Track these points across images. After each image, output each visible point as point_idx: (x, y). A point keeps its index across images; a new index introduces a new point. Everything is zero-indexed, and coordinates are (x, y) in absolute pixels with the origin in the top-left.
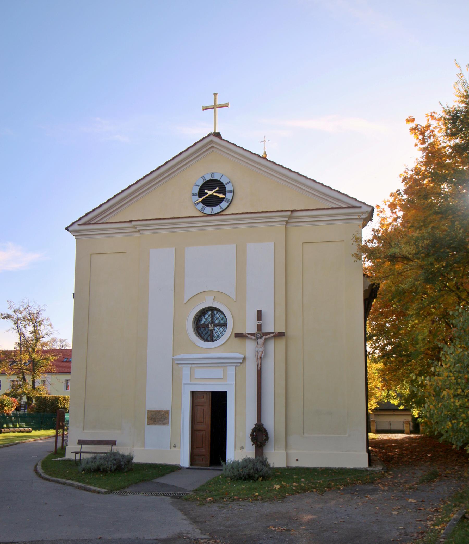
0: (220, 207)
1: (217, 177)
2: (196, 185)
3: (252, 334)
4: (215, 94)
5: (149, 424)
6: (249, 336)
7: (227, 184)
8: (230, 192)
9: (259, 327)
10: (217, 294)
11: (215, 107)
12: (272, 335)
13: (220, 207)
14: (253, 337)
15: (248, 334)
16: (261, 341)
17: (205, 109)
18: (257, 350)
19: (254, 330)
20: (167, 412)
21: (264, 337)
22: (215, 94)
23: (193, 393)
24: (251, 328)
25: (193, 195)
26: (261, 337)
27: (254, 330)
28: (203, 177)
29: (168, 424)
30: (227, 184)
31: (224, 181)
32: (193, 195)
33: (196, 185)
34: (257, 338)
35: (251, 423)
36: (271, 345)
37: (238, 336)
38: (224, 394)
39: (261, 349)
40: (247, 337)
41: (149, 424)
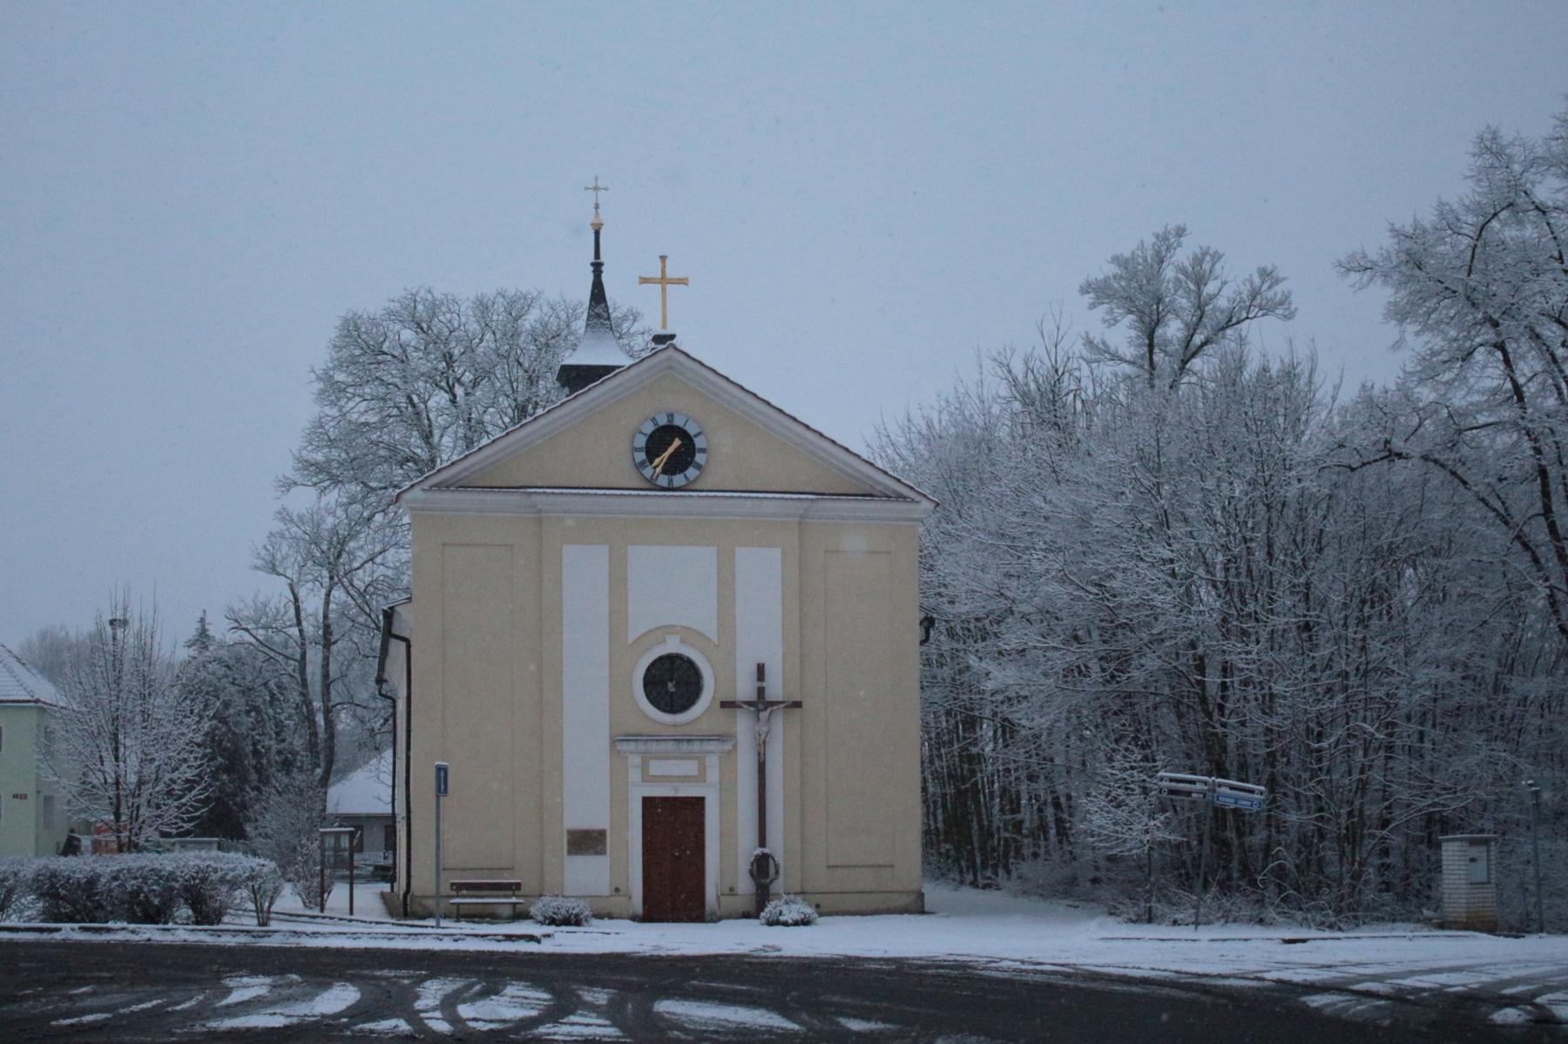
0: (685, 476)
1: (678, 422)
2: (641, 432)
3: (750, 704)
4: (663, 258)
5: (570, 853)
6: (746, 706)
7: (697, 435)
8: (703, 451)
9: (761, 691)
10: (688, 633)
11: (664, 280)
12: (782, 705)
13: (685, 476)
14: (752, 709)
15: (743, 702)
16: (764, 715)
17: (644, 281)
18: (757, 729)
19: (752, 696)
20: (602, 833)
21: (769, 710)
22: (663, 258)
23: (647, 802)
24: (745, 689)
25: (636, 450)
26: (766, 709)
27: (752, 696)
28: (653, 420)
29: (602, 852)
30: (697, 435)
31: (691, 429)
32: (636, 450)
33: (641, 432)
34: (759, 711)
35: (747, 847)
36: (778, 722)
37: (724, 705)
38: (699, 802)
39: (765, 729)
40: (741, 707)
41: (570, 853)
